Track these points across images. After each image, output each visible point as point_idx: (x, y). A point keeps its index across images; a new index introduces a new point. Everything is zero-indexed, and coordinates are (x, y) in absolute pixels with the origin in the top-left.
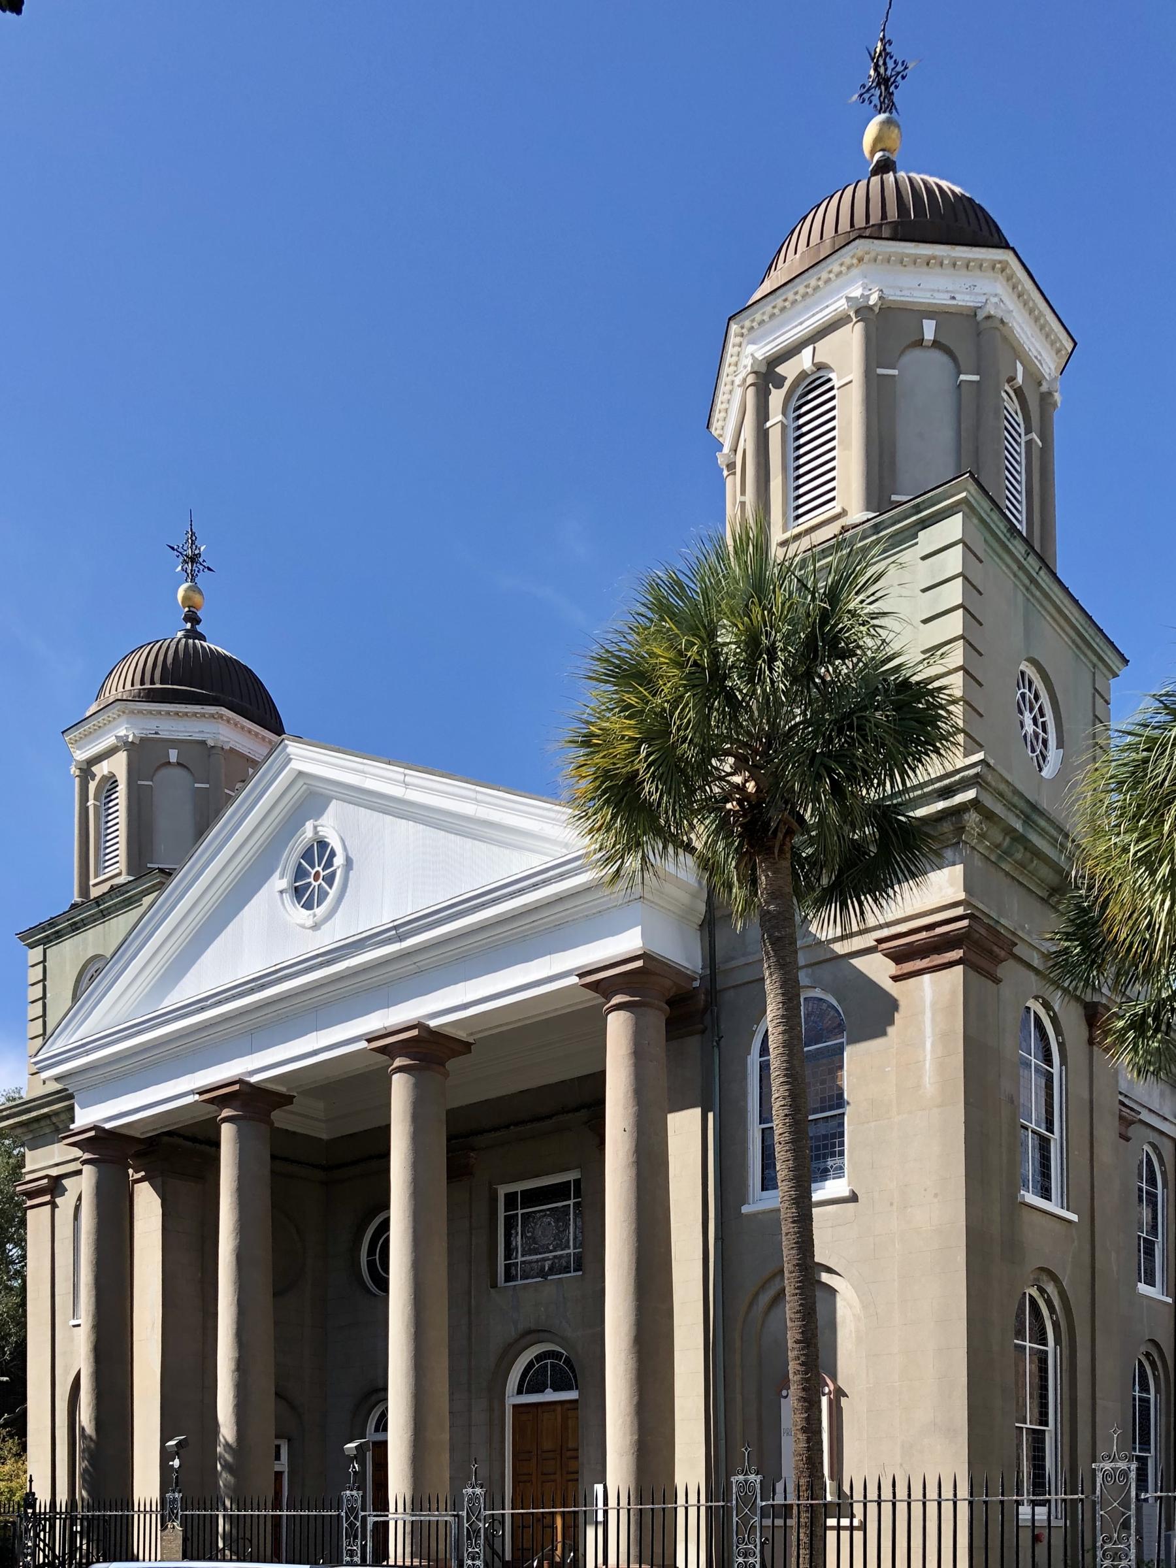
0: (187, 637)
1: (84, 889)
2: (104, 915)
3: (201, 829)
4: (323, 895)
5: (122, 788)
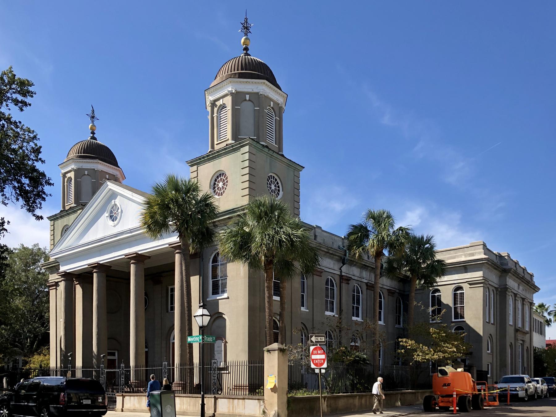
0: (91, 139)
1: (64, 207)
2: (68, 214)
3: (94, 193)
4: (116, 218)
5: (73, 181)
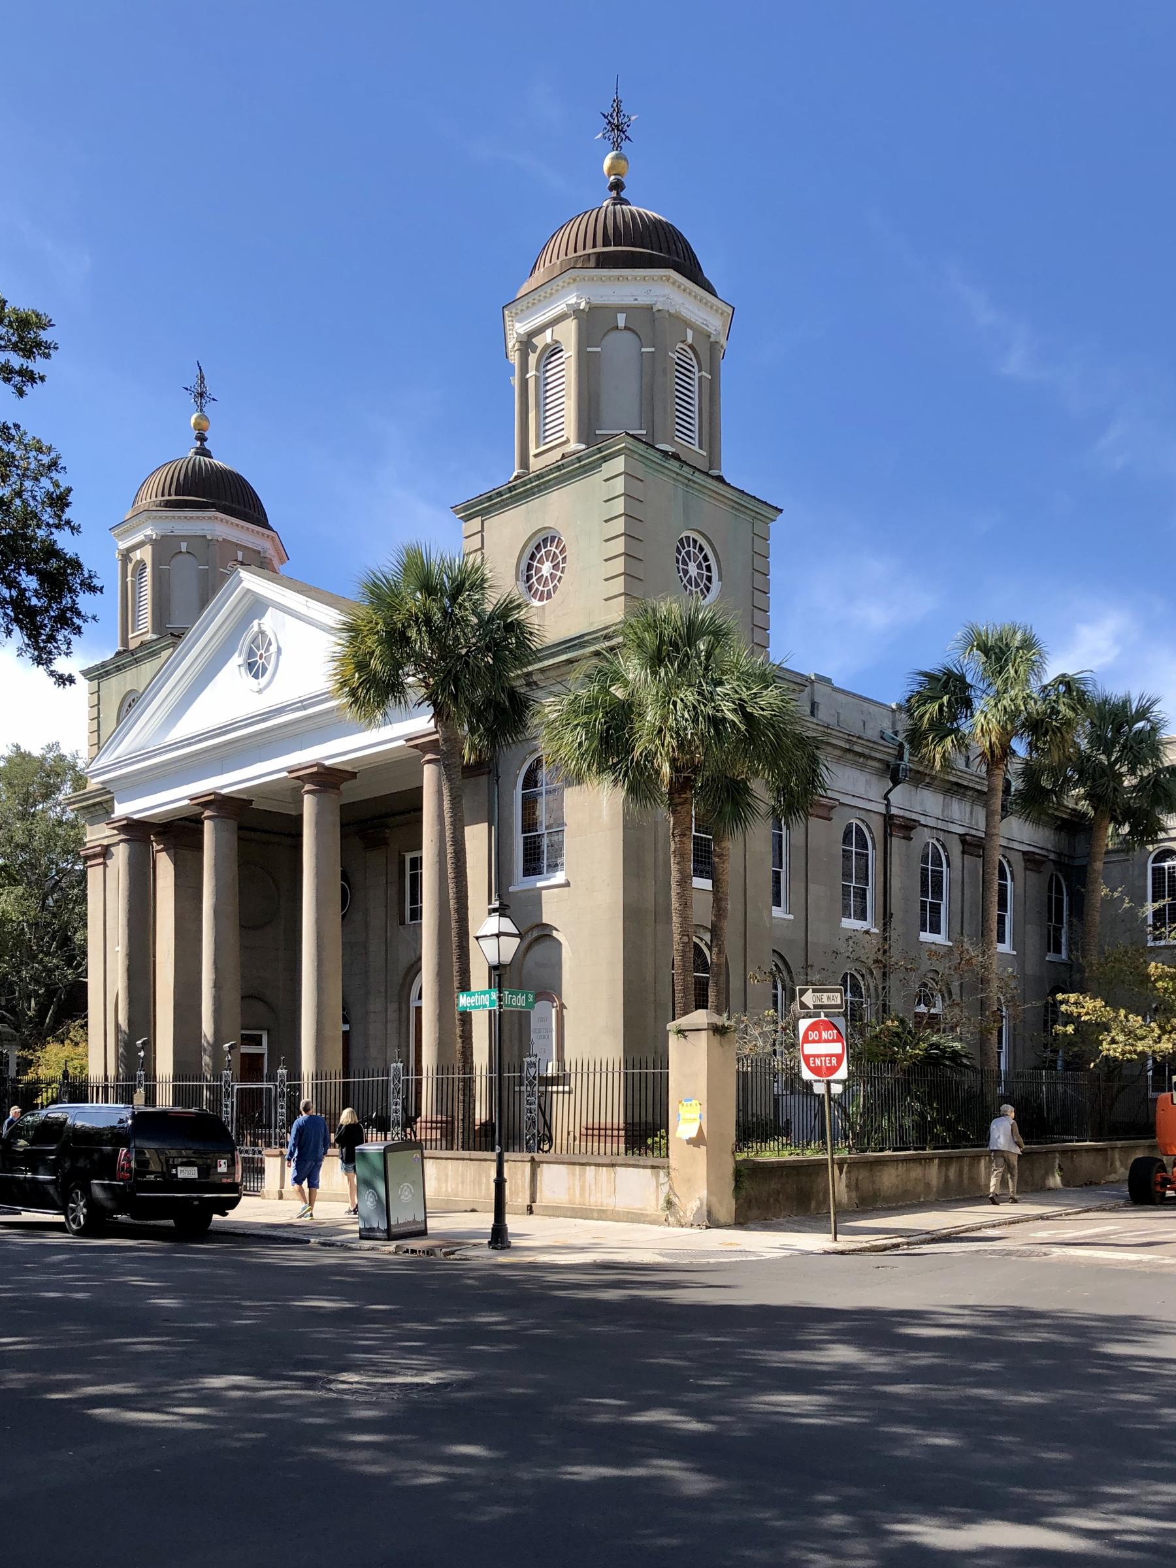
3: (204, 602)
4: (265, 670)
5: (149, 570)
